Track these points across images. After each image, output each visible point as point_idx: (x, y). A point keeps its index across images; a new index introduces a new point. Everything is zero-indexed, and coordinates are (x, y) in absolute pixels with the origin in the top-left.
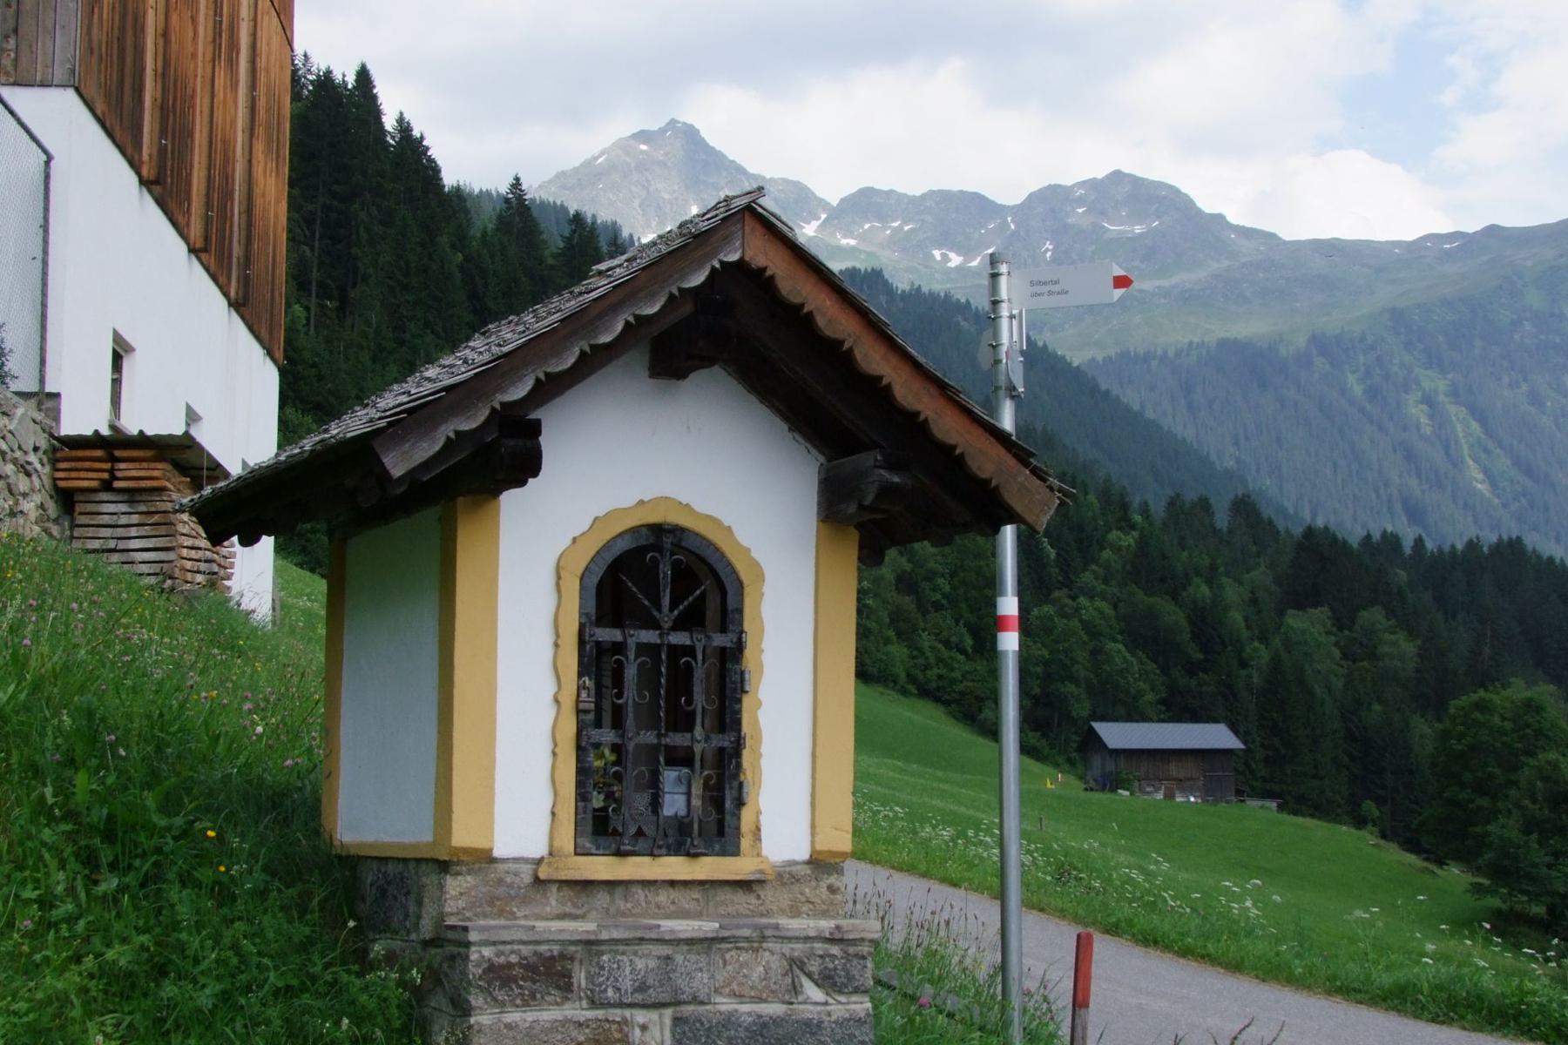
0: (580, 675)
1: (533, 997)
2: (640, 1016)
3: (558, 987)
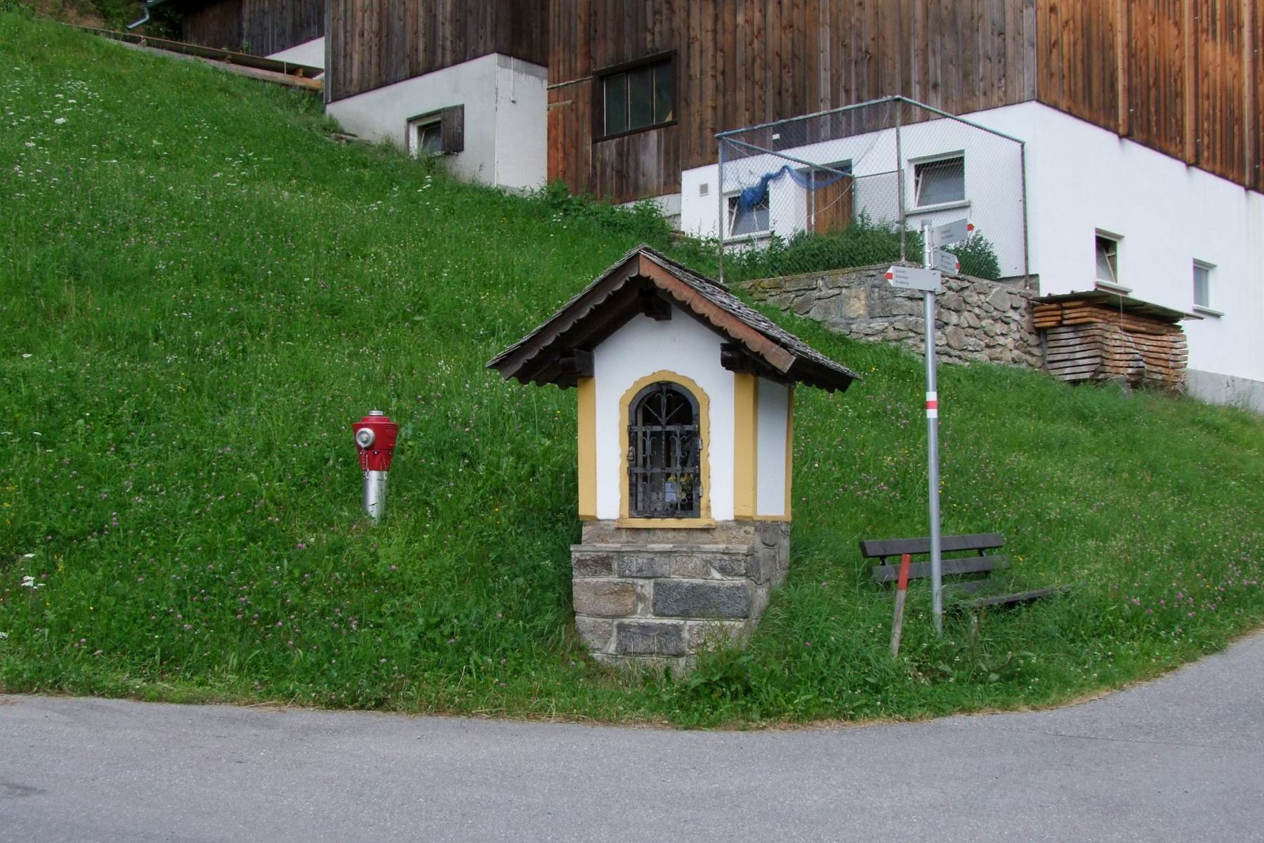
2: (641, 582)
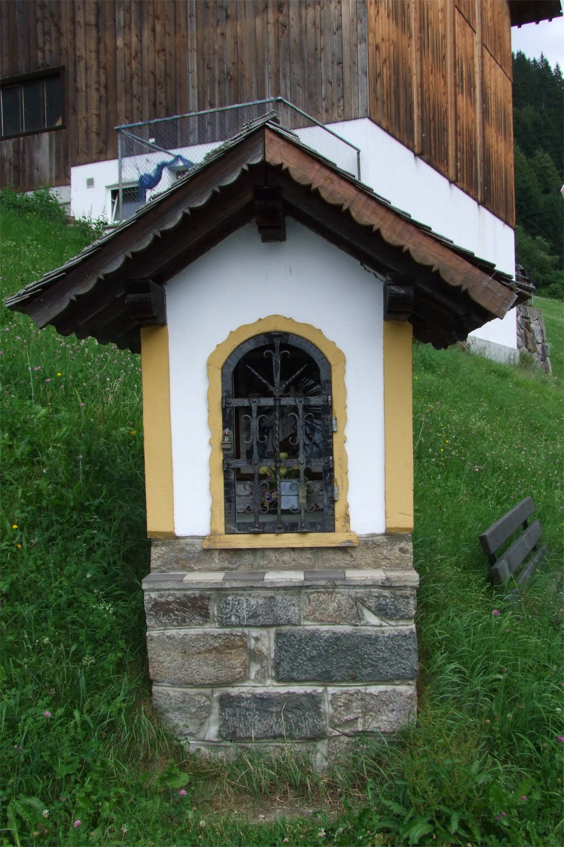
0: (224, 428)
1: (184, 621)
2: (255, 632)
3: (200, 615)
